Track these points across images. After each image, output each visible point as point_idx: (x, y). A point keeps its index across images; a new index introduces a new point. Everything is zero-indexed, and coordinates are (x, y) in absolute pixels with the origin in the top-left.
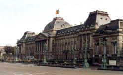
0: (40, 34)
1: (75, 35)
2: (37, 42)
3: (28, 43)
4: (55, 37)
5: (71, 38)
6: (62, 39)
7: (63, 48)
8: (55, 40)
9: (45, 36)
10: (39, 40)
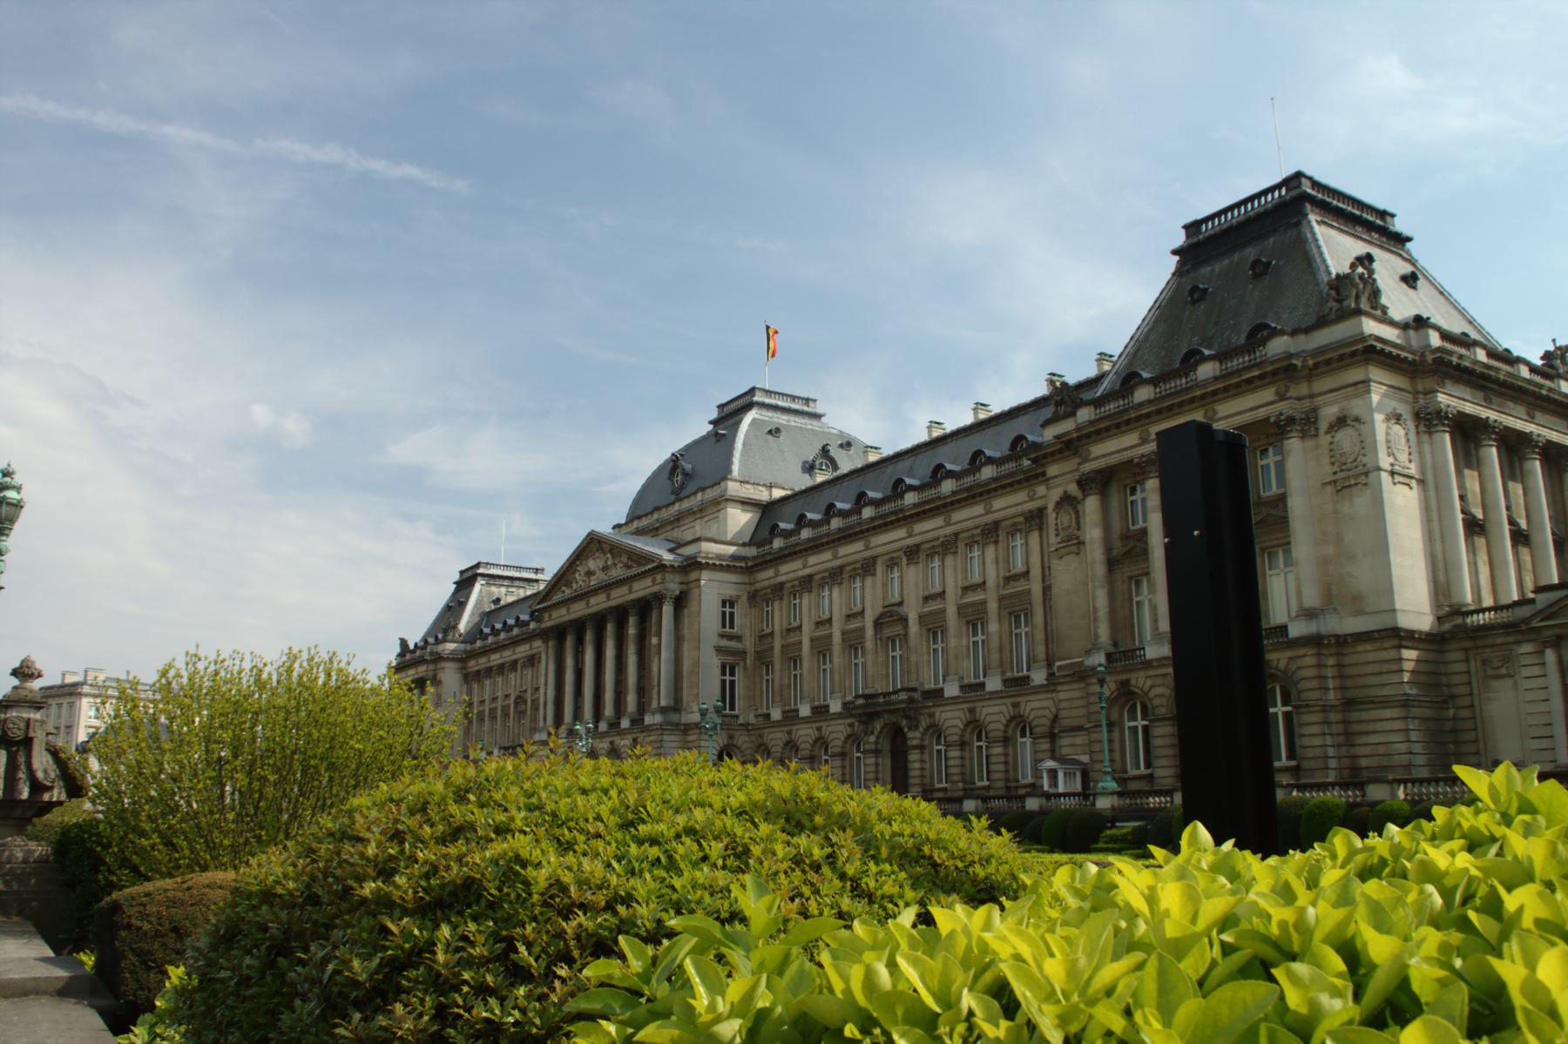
0: (593, 544)
1: (1008, 504)
2: (558, 634)
5: (947, 546)
6: (835, 576)
8: (753, 597)
9: (639, 558)
10: (579, 610)
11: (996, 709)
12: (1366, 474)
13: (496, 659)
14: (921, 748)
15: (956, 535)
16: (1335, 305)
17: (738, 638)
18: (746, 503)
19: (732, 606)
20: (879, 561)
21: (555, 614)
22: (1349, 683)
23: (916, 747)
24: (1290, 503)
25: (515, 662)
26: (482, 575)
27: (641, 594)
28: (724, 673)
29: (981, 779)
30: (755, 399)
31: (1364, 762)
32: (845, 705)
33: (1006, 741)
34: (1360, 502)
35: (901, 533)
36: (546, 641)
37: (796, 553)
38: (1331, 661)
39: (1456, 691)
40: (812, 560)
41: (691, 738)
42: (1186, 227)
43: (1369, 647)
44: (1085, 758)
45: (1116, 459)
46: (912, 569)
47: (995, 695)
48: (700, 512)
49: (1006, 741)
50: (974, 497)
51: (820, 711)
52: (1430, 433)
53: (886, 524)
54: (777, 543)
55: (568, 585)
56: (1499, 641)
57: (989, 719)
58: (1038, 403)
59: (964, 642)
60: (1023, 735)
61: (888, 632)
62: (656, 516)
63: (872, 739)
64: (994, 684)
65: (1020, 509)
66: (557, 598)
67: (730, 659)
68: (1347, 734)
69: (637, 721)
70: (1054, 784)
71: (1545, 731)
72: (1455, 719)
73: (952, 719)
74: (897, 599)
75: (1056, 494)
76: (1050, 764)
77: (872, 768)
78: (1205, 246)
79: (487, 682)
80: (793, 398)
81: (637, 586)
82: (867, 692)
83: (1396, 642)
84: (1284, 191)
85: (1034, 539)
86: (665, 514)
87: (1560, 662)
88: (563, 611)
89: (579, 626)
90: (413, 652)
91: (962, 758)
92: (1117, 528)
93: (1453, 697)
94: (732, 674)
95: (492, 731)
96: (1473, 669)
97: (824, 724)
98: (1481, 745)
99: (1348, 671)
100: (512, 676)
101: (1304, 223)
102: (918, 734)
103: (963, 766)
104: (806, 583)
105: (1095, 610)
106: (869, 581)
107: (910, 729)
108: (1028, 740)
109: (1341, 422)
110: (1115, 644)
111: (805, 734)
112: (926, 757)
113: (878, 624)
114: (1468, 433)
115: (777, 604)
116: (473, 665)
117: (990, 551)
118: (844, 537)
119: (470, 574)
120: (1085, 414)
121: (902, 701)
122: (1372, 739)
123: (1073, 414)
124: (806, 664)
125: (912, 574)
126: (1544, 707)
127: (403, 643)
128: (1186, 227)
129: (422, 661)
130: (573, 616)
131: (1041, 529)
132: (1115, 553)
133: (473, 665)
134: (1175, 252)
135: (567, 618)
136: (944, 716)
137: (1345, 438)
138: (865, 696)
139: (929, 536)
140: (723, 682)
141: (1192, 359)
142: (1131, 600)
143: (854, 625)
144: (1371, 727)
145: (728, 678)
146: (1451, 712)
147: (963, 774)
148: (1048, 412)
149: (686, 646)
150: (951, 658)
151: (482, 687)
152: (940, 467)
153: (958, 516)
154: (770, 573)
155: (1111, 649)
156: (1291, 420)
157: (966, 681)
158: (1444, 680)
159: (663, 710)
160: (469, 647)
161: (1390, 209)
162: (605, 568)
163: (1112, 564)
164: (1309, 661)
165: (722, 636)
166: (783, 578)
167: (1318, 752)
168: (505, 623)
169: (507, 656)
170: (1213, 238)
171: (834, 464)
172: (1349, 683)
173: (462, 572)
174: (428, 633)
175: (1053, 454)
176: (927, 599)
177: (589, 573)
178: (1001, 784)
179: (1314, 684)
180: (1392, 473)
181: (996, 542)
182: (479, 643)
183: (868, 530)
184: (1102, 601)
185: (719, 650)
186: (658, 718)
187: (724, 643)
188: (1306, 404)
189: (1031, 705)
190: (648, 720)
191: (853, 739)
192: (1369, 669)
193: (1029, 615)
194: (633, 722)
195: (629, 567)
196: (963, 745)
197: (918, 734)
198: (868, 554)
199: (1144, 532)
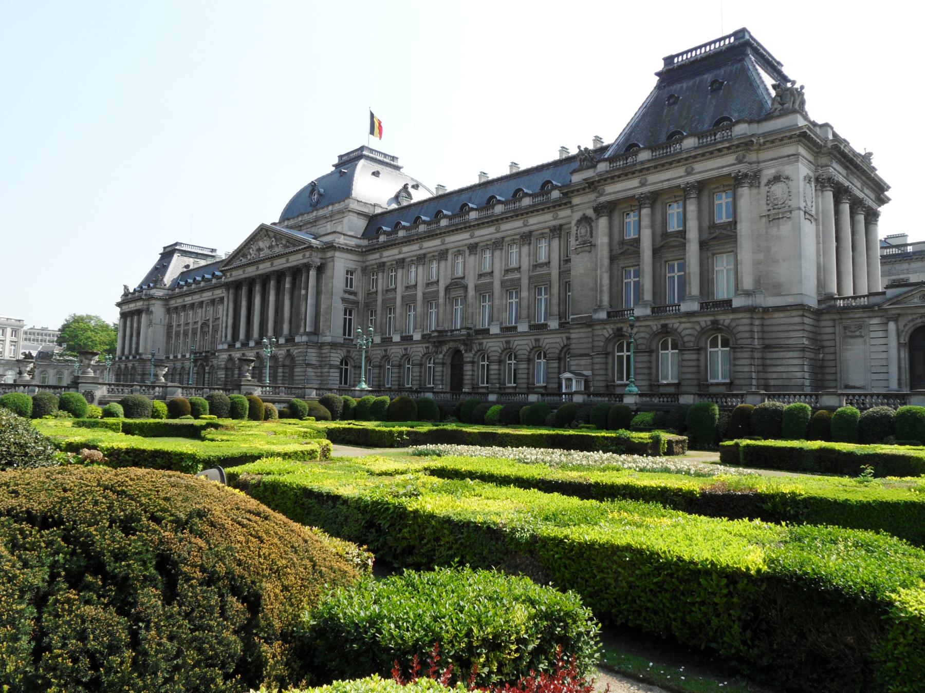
0: (263, 232)
2: (236, 286)
3: (179, 302)
4: (362, 252)
5: (497, 244)
6: (421, 259)
7: (426, 315)
8: (364, 270)
9: (292, 241)
10: (251, 272)
11: (524, 342)
12: (791, 212)
13: (188, 300)
14: (473, 363)
15: (503, 238)
16: (780, 107)
17: (355, 294)
18: (360, 214)
19: (352, 275)
20: (450, 252)
21: (234, 273)
22: (766, 336)
23: (469, 362)
24: (739, 227)
25: (202, 302)
26: (179, 250)
27: (295, 264)
28: (345, 314)
29: (510, 382)
30: (364, 153)
31: (772, 382)
32: (423, 336)
33: (529, 360)
34: (785, 228)
35: (465, 235)
36: (228, 290)
37: (395, 245)
38: (757, 322)
39: (825, 343)
40: (405, 249)
41: (324, 351)
42: (665, 59)
43: (782, 315)
44: (588, 373)
45: (621, 195)
46: (472, 257)
47: (523, 334)
48: (330, 217)
49: (529, 360)
50: (517, 216)
51: (407, 339)
52: (822, 191)
53: (457, 230)
54: (382, 238)
55: (244, 256)
56: (857, 316)
57: (518, 348)
58: (555, 164)
59: (504, 302)
60: (539, 358)
61: (453, 294)
62: (300, 219)
63: (441, 356)
64: (523, 327)
65: (547, 224)
66: (236, 263)
67: (350, 306)
68: (763, 365)
69: (290, 340)
70: (569, 386)
71: (884, 370)
72: (823, 360)
73: (494, 346)
74: (460, 274)
75: (578, 215)
76: (568, 375)
77: (439, 374)
78: (675, 74)
79: (182, 314)
80: (385, 155)
81: (291, 258)
82: (440, 328)
83: (800, 313)
84: (732, 39)
85: (555, 243)
86: (306, 218)
87: (898, 330)
88: (240, 272)
89: (251, 282)
90: (133, 293)
91: (499, 370)
92: (616, 237)
93: (823, 347)
94: (350, 315)
95: (185, 342)
96: (837, 332)
97: (409, 347)
98: (838, 375)
99: (766, 328)
100: (199, 311)
101: (746, 59)
102: (471, 355)
103: (499, 374)
104: (401, 263)
105: (601, 286)
106: (443, 264)
107: (466, 351)
108: (543, 361)
109: (777, 179)
110: (611, 306)
111: (396, 352)
112: (475, 369)
113: (447, 289)
114: (840, 192)
115: (380, 274)
116: (173, 303)
117: (525, 249)
118: (428, 237)
119: (170, 249)
120: (602, 167)
121: (463, 335)
122: (774, 369)
123: (594, 166)
124: (398, 311)
125: (472, 260)
126: (884, 355)
127: (126, 287)
128: (665, 59)
129: (140, 299)
130: (246, 276)
131: (560, 237)
132: (614, 253)
133: (173, 303)
134: (657, 74)
135: (243, 276)
136: (489, 345)
137: (778, 189)
138: (439, 332)
139: (486, 238)
140: (345, 319)
141: (674, 137)
142: (622, 281)
143: (432, 289)
144: (779, 362)
145: (348, 317)
146: (821, 356)
147: (499, 379)
148: (576, 165)
149: (323, 297)
150: (496, 314)
151: (179, 316)
152: (493, 197)
153: (504, 227)
154: (377, 256)
155: (610, 310)
156: (746, 176)
157: (504, 325)
158: (818, 337)
159: (308, 334)
160: (170, 292)
161: (782, 62)
162: (271, 247)
163: (612, 259)
164: (745, 321)
165: (345, 292)
166: (385, 260)
167: (746, 375)
168: (195, 279)
169: (196, 298)
170: (684, 67)
171: (409, 196)
172: (766, 336)
173: (165, 248)
174: (142, 283)
175: (578, 190)
176: (480, 276)
177: (259, 250)
178: (525, 386)
179: (748, 335)
180: (805, 212)
181: (530, 244)
182: (177, 290)
183: (444, 233)
184: (606, 281)
185: (344, 300)
186: (305, 339)
187: (347, 296)
188: (754, 166)
189: (547, 341)
190: (297, 339)
191: (427, 356)
192: (780, 328)
193: (548, 289)
194: (287, 341)
195: (288, 247)
196: (500, 362)
197: (471, 355)
198: (443, 247)
199: (637, 241)
